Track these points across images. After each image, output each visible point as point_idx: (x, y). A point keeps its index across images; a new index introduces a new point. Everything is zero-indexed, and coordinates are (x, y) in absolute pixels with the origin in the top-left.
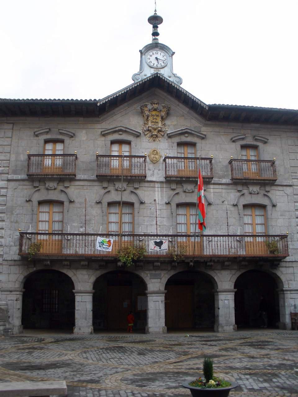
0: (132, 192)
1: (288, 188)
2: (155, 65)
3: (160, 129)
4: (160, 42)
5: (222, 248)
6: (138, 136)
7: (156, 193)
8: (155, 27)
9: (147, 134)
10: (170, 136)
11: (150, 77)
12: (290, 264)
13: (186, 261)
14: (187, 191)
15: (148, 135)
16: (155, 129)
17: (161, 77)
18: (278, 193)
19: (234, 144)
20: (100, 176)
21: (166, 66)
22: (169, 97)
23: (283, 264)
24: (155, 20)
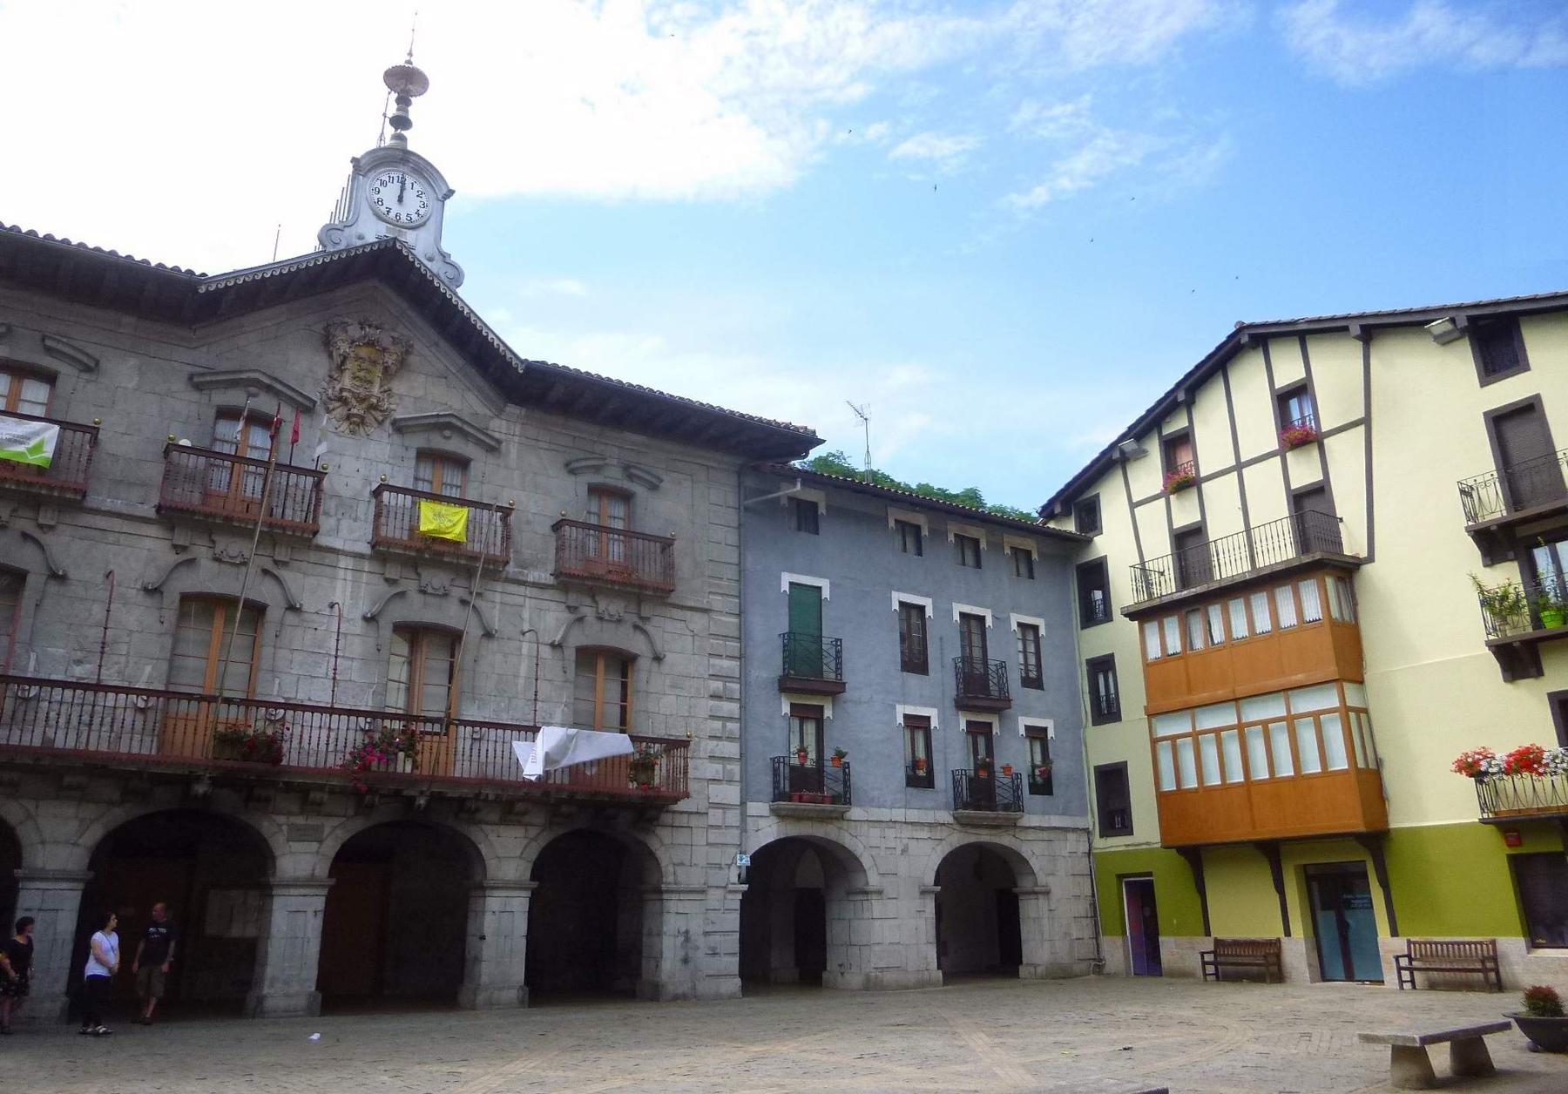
0: (266, 572)
1: (697, 616)
2: (392, 215)
4: (410, 147)
5: (498, 759)
6: (306, 408)
7: (339, 584)
8: (404, 101)
10: (400, 428)
11: (372, 244)
13: (405, 793)
14: (430, 590)
18: (670, 626)
19: (573, 478)
20: (170, 508)
21: (423, 224)
23: (666, 818)
24: (406, 82)
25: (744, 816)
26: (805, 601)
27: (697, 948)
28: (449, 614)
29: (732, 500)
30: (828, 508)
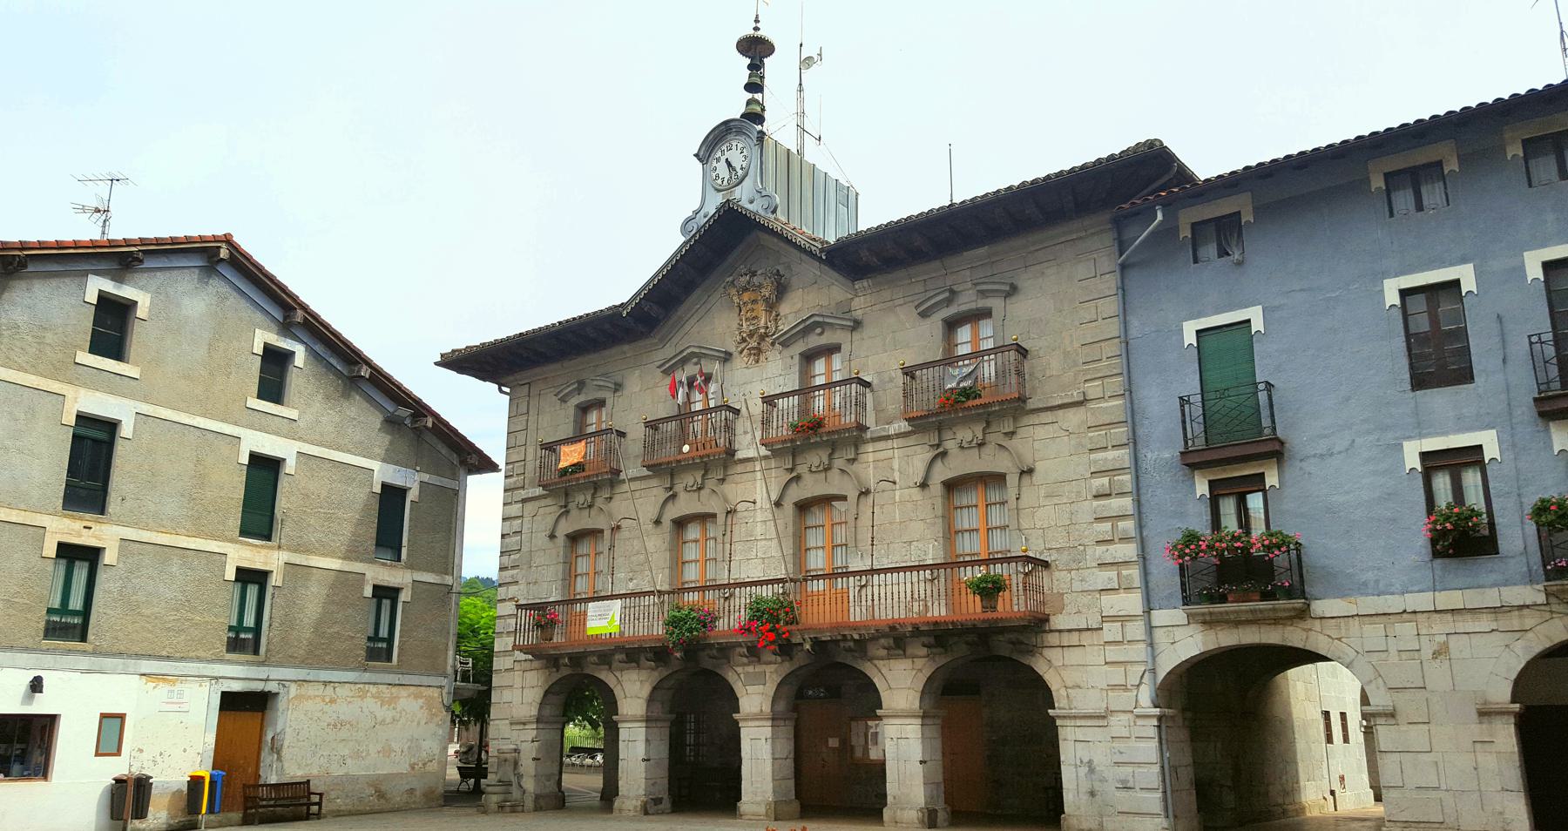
6: (727, 357)
8: (756, 67)
10: (785, 344)
12: (1074, 638)
18: (1040, 432)
25: (1150, 629)
26: (1225, 349)
27: (1103, 780)
30: (1257, 211)
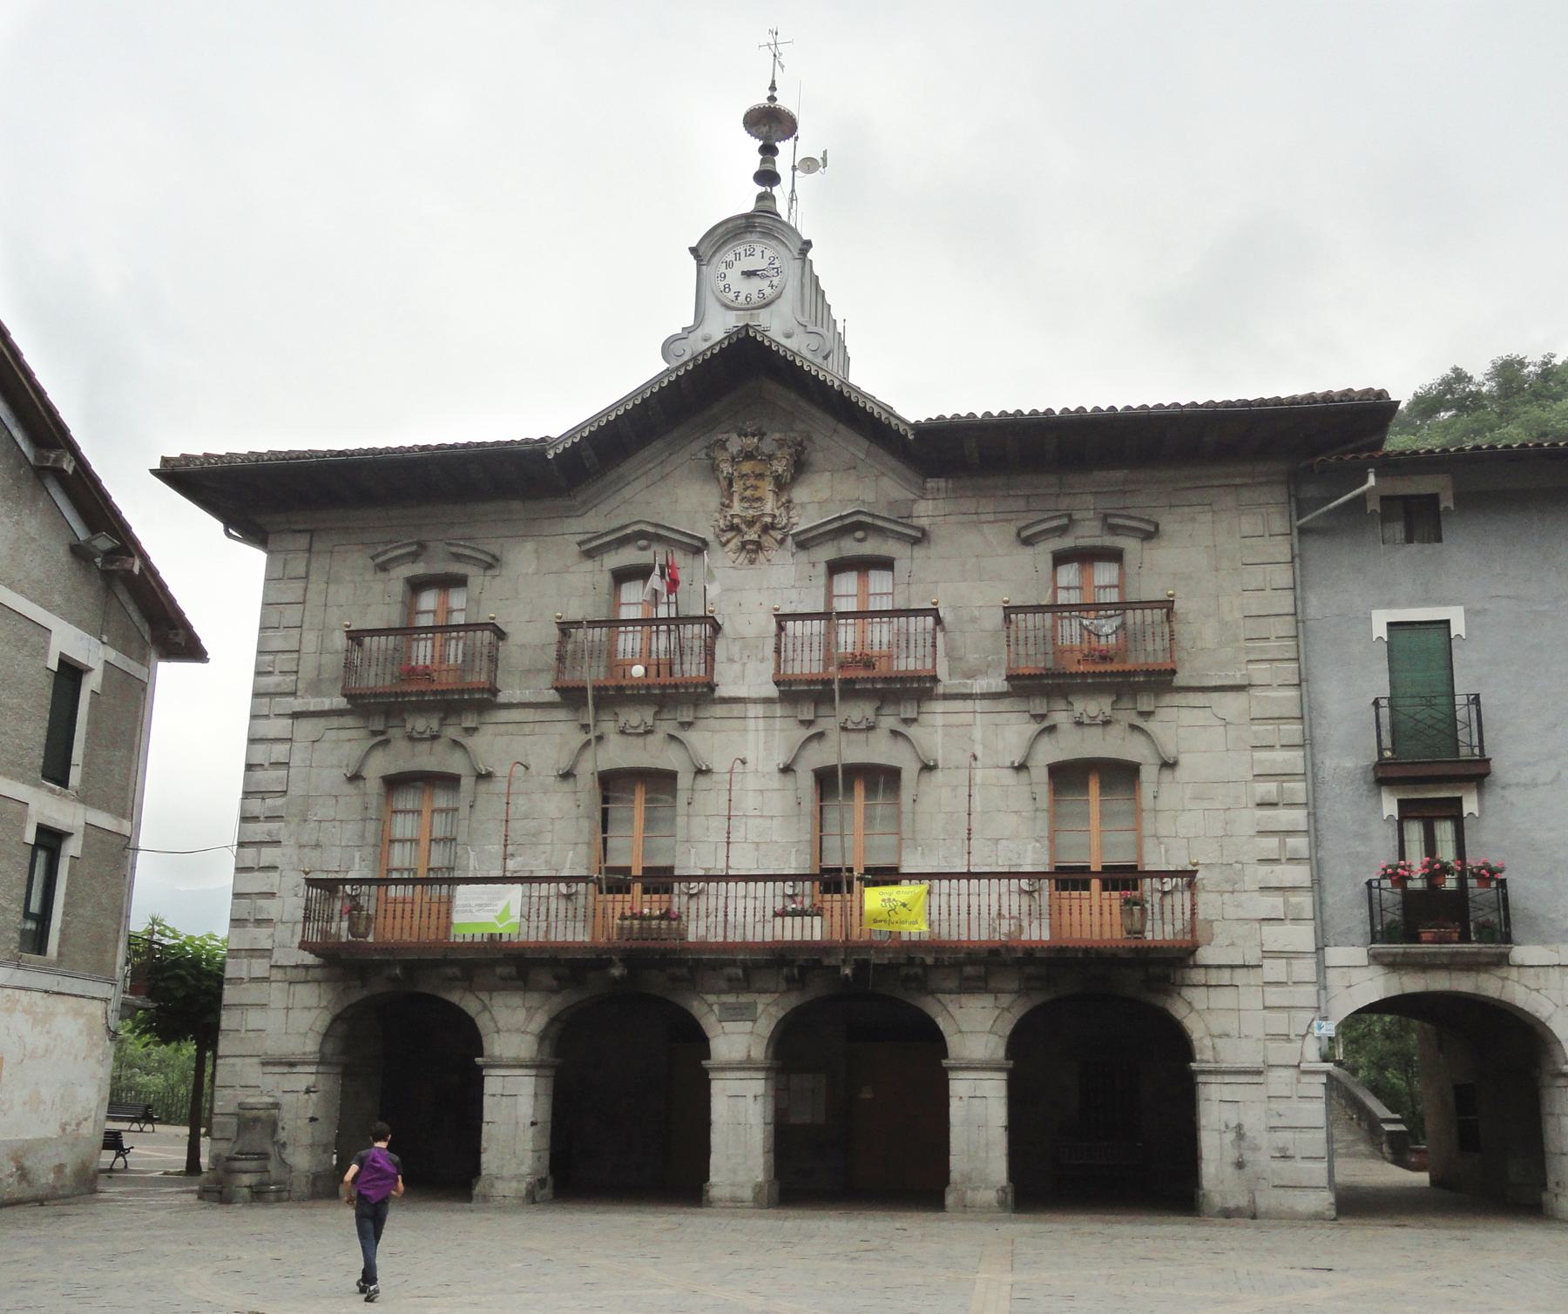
1: (1230, 697)
2: (742, 298)
3: (768, 520)
6: (697, 548)
7: (751, 736)
8: (768, 151)
9: (728, 541)
10: (805, 543)
11: (721, 342)
12: (1225, 977)
15: (732, 545)
16: (751, 523)
17: (759, 338)
18: (1187, 716)
19: (1029, 551)
22: (803, 404)
25: (1322, 968)
26: (1421, 649)
27: (1256, 1149)
28: (878, 750)
29: (1279, 523)
